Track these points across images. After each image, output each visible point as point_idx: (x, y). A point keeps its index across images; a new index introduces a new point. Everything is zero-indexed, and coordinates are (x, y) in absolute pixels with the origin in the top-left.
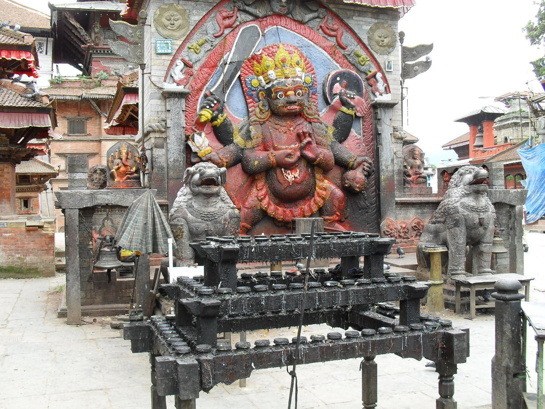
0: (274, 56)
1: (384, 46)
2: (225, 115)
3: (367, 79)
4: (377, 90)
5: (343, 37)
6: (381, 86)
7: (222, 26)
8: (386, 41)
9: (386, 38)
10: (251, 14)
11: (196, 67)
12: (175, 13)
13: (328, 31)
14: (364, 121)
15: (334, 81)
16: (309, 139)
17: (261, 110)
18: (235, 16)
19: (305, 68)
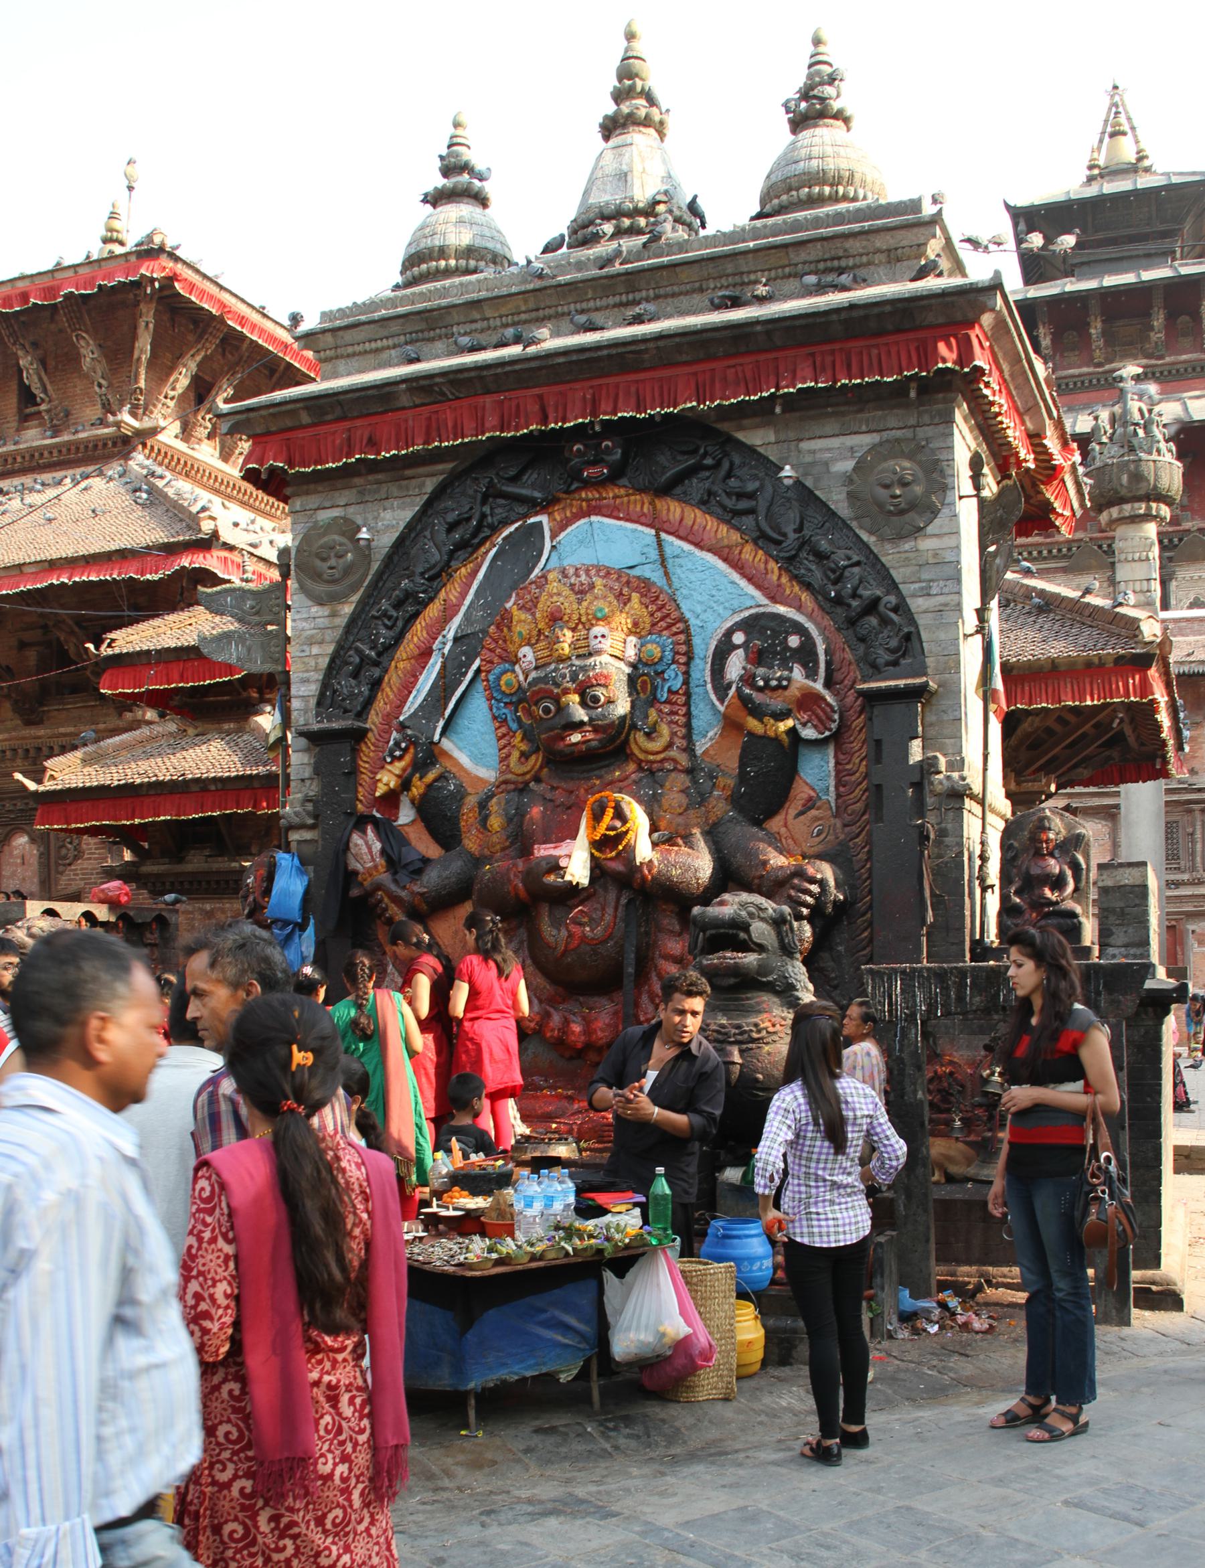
1: (902, 512)
2: (431, 776)
12: (336, 537)
13: (730, 503)
17: (523, 754)
18: (477, 516)
19: (648, 620)
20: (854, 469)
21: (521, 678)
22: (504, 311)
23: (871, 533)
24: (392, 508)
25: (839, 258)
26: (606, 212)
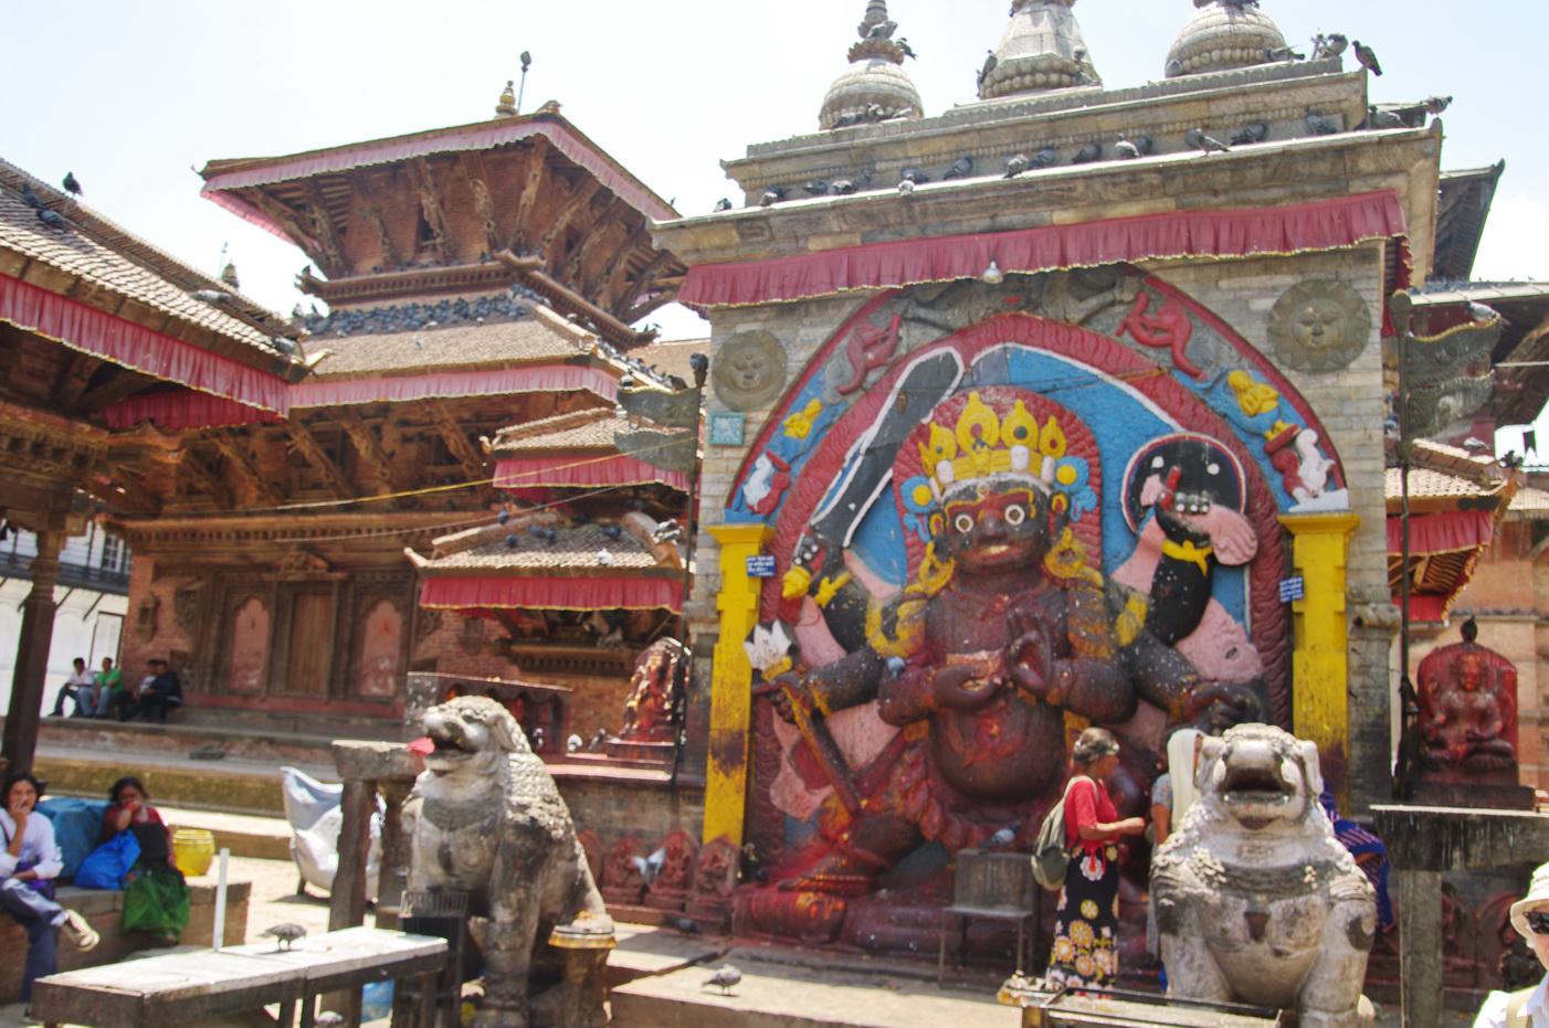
0: (955, 421)
2: (841, 579)
3: (1271, 453)
4: (1298, 482)
5: (1189, 344)
6: (1313, 468)
7: (861, 366)
8: (1330, 333)
9: (1327, 322)
10: (934, 325)
11: (798, 468)
13: (1144, 334)
14: (1253, 576)
15: (1143, 470)
16: (1032, 635)
20: (1277, 306)
21: (936, 491)
22: (925, 150)
23: (1292, 367)
24: (812, 325)
25: (1258, 112)
26: (1025, 68)
